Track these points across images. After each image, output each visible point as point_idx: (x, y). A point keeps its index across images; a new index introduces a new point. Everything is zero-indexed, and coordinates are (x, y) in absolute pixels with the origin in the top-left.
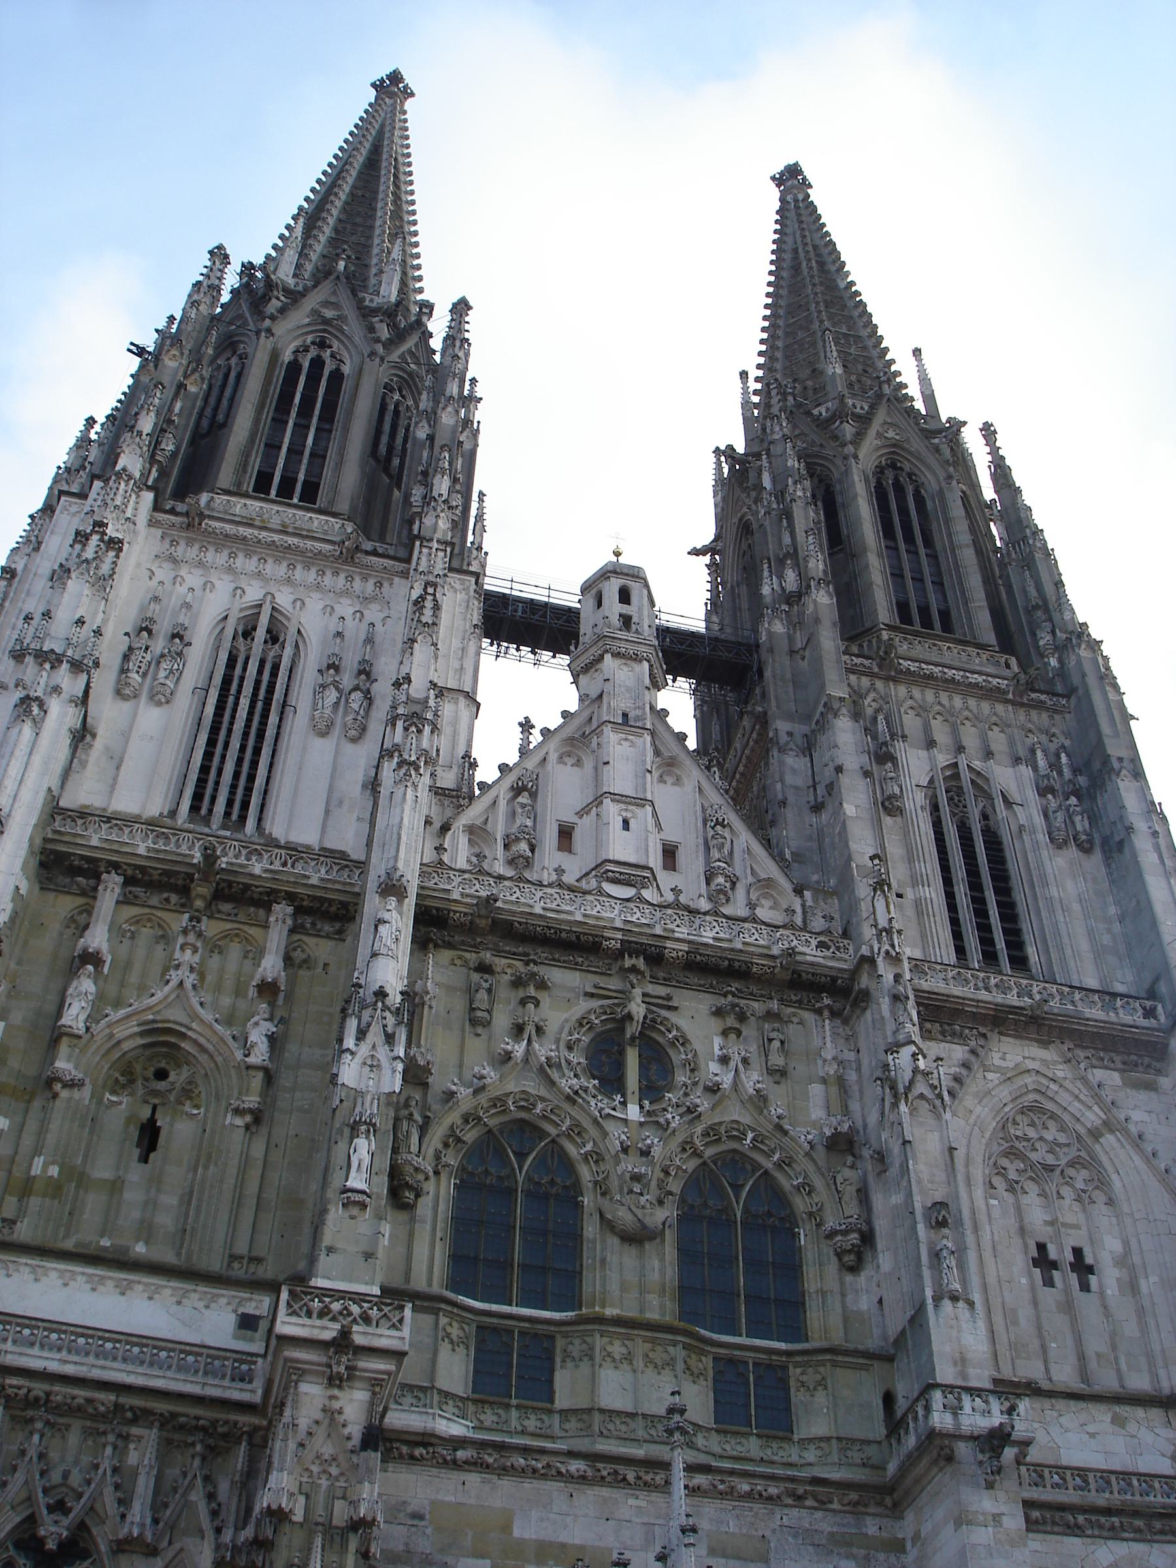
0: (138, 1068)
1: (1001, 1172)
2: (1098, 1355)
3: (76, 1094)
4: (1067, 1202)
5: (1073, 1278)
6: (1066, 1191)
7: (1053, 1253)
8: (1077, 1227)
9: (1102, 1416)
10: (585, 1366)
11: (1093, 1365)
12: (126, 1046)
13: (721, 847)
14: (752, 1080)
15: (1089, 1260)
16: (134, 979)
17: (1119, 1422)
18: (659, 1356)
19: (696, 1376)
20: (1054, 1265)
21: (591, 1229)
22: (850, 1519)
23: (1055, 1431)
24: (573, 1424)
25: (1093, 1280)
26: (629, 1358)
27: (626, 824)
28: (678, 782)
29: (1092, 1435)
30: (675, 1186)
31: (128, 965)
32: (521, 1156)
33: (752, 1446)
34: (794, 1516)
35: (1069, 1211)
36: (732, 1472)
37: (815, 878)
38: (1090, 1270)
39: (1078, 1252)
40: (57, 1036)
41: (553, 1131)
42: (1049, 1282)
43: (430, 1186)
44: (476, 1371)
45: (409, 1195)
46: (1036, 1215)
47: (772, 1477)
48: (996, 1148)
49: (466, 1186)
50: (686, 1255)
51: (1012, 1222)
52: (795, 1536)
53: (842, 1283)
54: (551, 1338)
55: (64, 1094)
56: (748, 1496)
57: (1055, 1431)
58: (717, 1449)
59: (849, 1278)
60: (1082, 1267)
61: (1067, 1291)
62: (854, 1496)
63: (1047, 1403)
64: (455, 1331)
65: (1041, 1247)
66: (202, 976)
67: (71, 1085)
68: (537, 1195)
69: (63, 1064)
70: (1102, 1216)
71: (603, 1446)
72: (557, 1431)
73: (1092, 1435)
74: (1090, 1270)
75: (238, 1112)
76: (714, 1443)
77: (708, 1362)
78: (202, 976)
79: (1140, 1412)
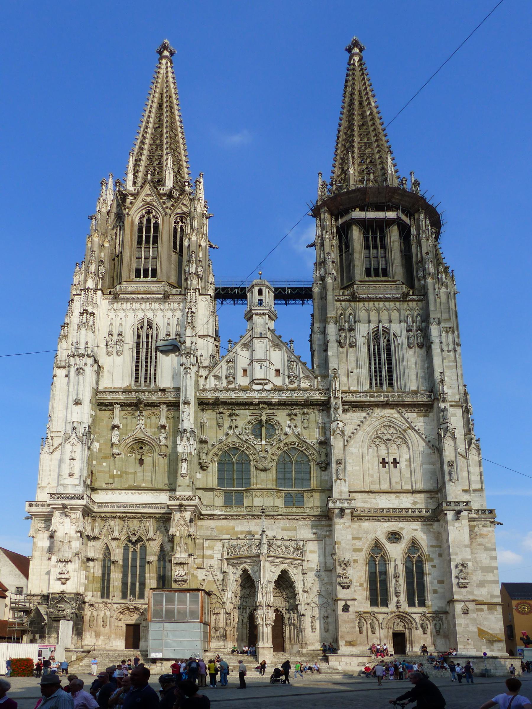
0: (135, 448)
1: (374, 443)
2: (396, 482)
3: (121, 456)
4: (394, 448)
5: (392, 466)
6: (394, 445)
7: (387, 460)
8: (396, 453)
9: (393, 496)
10: (251, 498)
11: (394, 484)
12: (130, 444)
13: (292, 369)
14: (299, 429)
15: (398, 461)
16: (129, 428)
17: (396, 497)
18: (269, 494)
19: (279, 497)
20: (387, 463)
21: (253, 469)
22: (318, 522)
23: (378, 500)
24: (248, 509)
25: (398, 465)
26: (261, 496)
27: (261, 366)
28: (280, 349)
29: (389, 500)
30: (276, 458)
31: (127, 425)
32: (234, 455)
33: (295, 510)
34: (303, 522)
35: (393, 449)
36: (287, 515)
37: (323, 372)
38: (398, 463)
39: (395, 459)
40: (112, 445)
41: (242, 449)
42: (384, 467)
43: (211, 465)
44: (224, 501)
45: (205, 468)
46: (383, 451)
47: (297, 516)
48: (373, 437)
49: (220, 463)
50: (278, 472)
51: (376, 454)
52: (303, 526)
53: (321, 474)
54: (243, 493)
55: (117, 456)
56: (292, 519)
57: (378, 500)
58: (285, 511)
59: (323, 473)
60: (395, 462)
61: (389, 469)
62: (319, 517)
63: (377, 494)
64: (218, 494)
65: (384, 459)
66: (146, 425)
67: (118, 455)
68: (239, 463)
69: (115, 451)
70: (404, 450)
71: (254, 513)
72: (245, 511)
73: (389, 500)
74: (398, 463)
75: (160, 455)
76: (284, 510)
77: (283, 494)
78: (146, 425)
79: (405, 494)
